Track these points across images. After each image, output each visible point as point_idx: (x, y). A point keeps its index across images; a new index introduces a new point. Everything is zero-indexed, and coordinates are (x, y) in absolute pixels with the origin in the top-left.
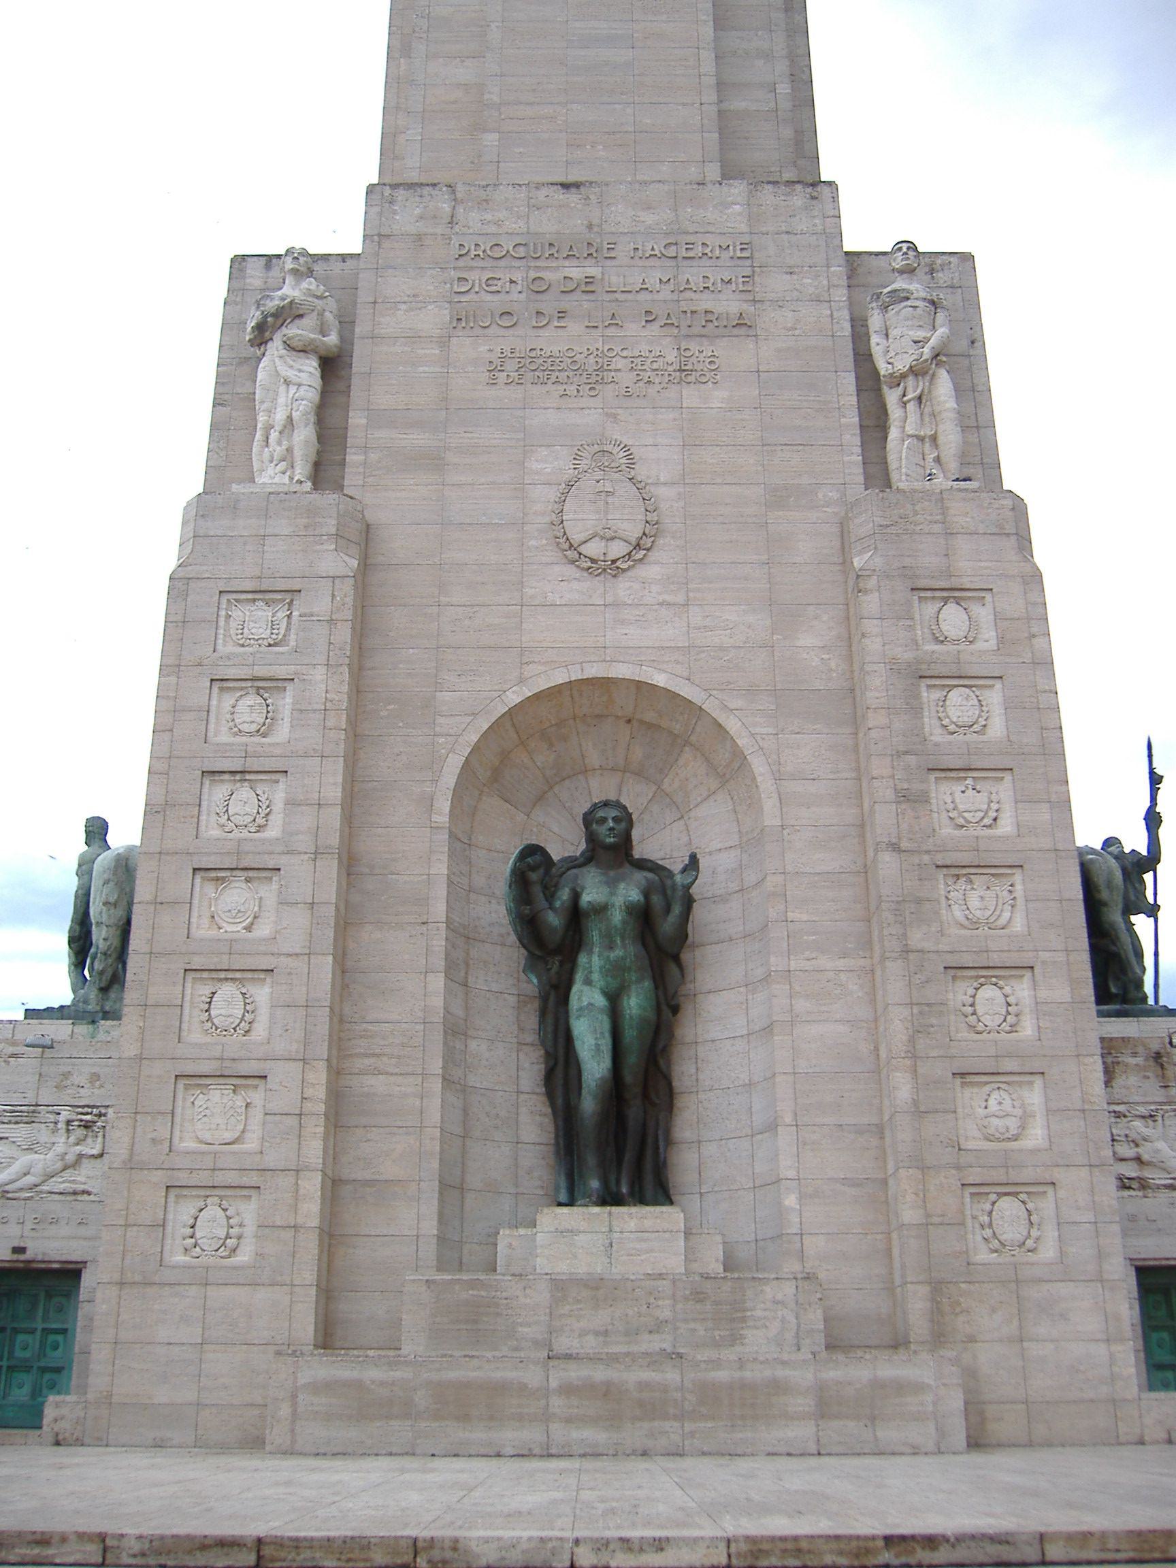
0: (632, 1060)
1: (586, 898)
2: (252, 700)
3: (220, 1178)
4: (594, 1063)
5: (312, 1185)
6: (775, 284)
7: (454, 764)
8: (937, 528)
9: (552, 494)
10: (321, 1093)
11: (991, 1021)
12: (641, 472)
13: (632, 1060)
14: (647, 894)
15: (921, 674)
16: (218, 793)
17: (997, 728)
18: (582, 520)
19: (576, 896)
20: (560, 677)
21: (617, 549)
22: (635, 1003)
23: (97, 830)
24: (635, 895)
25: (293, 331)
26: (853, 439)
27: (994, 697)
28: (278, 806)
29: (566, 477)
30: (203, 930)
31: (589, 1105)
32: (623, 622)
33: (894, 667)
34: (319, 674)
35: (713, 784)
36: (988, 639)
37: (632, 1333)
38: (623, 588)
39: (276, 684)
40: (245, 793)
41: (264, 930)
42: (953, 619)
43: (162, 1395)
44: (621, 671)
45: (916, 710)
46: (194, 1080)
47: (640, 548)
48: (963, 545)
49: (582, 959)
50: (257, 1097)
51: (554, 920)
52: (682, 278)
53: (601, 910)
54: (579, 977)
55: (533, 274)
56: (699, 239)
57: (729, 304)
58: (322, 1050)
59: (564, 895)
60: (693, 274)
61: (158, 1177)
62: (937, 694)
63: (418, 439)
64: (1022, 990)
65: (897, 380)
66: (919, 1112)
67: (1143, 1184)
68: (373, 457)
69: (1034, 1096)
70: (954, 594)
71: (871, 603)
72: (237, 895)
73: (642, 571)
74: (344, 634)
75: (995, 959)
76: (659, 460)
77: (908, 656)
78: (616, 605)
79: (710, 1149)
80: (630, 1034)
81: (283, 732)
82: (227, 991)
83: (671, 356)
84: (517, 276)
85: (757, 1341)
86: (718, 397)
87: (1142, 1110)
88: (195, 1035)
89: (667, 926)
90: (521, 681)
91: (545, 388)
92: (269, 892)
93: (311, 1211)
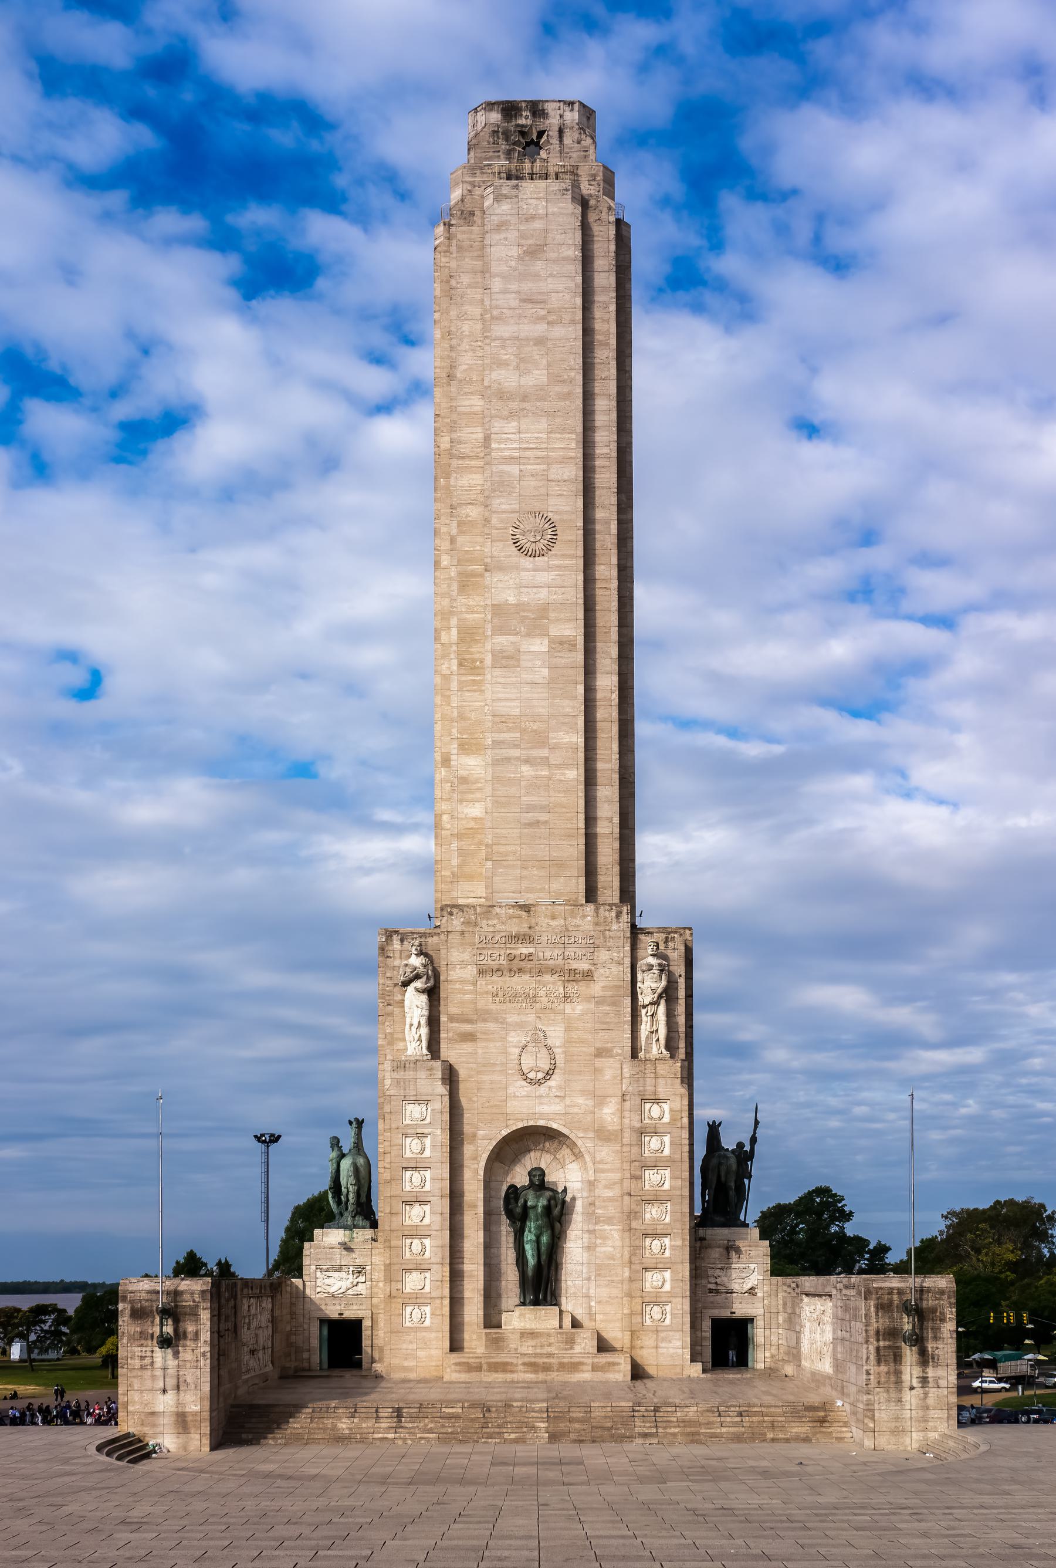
0: (544, 1257)
1: (529, 1203)
2: (416, 1141)
3: (418, 1301)
4: (531, 1261)
5: (447, 1302)
6: (603, 955)
7: (485, 1156)
8: (653, 1075)
9: (517, 1051)
10: (448, 1274)
11: (656, 1251)
12: (549, 1042)
13: (544, 1257)
14: (549, 1201)
15: (642, 1132)
16: (408, 1174)
17: (667, 1152)
18: (528, 1062)
19: (526, 1202)
20: (520, 1125)
21: (540, 1075)
22: (544, 1239)
23: (335, 1143)
24: (545, 1203)
25: (419, 984)
26: (628, 1028)
27: (667, 1139)
28: (428, 1179)
29: (521, 1045)
30: (408, 1222)
31: (530, 1273)
32: (542, 1104)
33: (633, 1128)
34: (439, 1132)
35: (574, 1158)
36: (667, 1119)
37: (542, 1346)
38: (542, 1090)
39: (424, 1135)
40: (416, 1175)
41: (427, 1221)
42: (655, 1111)
43: (406, 1364)
44: (541, 1123)
45: (640, 1144)
46: (409, 1270)
47: (549, 1075)
48: (661, 1081)
49: (528, 1223)
50: (428, 1275)
51: (519, 1210)
52: (567, 953)
53: (534, 1207)
54: (527, 1229)
55: (508, 952)
56: (573, 934)
57: (584, 966)
58: (448, 1261)
59: (521, 1202)
60: (570, 951)
61: (400, 1300)
62: (647, 1139)
63: (467, 1027)
64: (667, 1241)
65: (644, 1007)
66: (631, 1280)
67: (717, 1292)
68: (451, 1035)
69: (667, 1275)
70: (657, 1101)
71: (627, 1104)
72: (416, 1211)
73: (549, 1083)
74: (446, 1117)
75: (659, 1231)
76: (556, 1036)
77: (638, 1125)
78: (541, 1096)
79: (569, 1283)
80: (543, 1249)
81: (427, 1153)
82: (416, 1242)
83: (561, 990)
84: (502, 953)
85: (578, 1349)
86: (577, 1009)
87: (719, 1266)
88: (408, 1255)
89: (556, 1211)
90: (507, 1126)
91: (513, 1005)
92: (427, 1208)
93: (446, 1310)
